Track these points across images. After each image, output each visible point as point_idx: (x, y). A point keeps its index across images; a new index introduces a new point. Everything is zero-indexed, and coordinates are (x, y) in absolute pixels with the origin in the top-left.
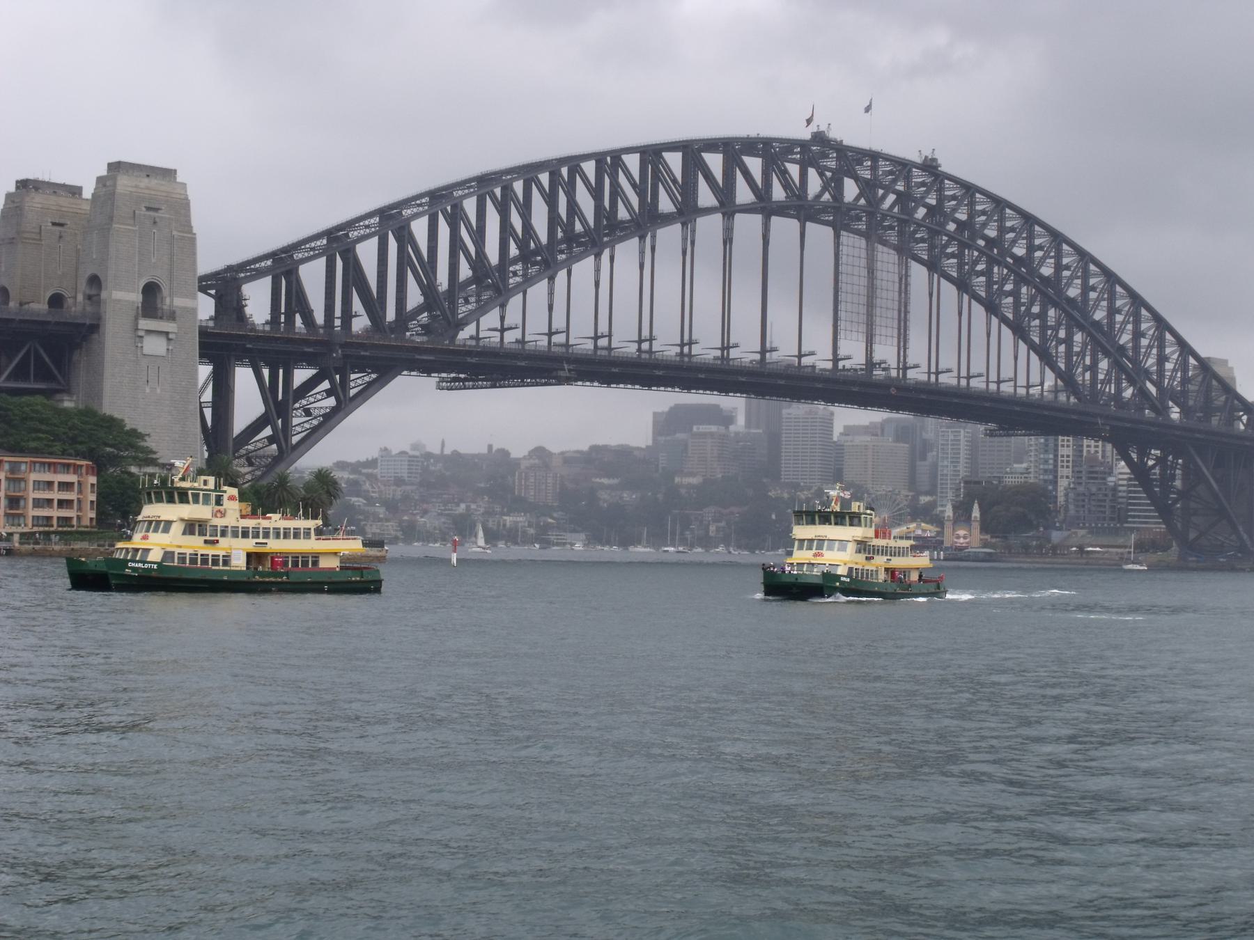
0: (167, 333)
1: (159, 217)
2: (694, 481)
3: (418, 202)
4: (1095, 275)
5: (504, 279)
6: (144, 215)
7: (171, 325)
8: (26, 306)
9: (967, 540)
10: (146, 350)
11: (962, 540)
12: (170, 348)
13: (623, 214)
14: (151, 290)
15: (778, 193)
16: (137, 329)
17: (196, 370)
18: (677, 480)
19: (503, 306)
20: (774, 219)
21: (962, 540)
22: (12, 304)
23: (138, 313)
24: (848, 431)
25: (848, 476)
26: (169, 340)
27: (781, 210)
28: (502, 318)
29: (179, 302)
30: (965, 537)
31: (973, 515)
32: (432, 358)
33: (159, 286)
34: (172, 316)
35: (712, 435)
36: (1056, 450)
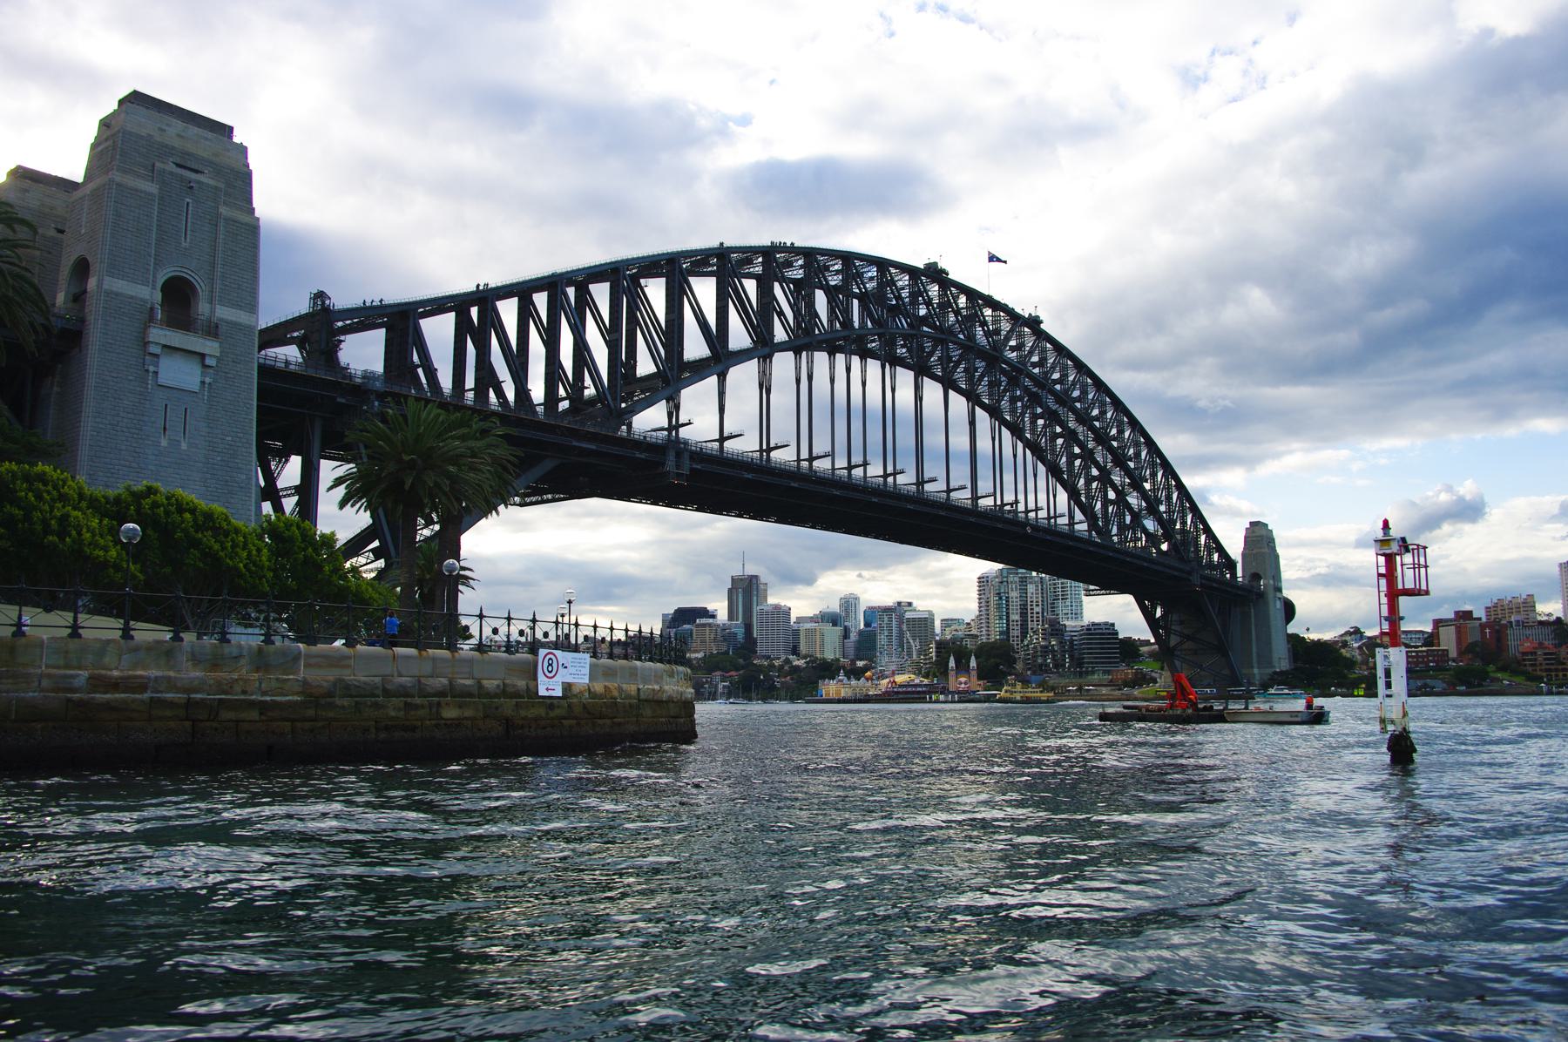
0: (203, 356)
1: (199, 182)
2: (700, 655)
6: (171, 173)
7: (209, 343)
10: (162, 380)
11: (963, 686)
12: (208, 380)
16: (146, 344)
18: (688, 655)
21: (963, 686)
24: (800, 620)
25: (803, 649)
26: (205, 366)
29: (224, 313)
31: (971, 665)
32: (594, 447)
35: (710, 625)
36: (1008, 617)
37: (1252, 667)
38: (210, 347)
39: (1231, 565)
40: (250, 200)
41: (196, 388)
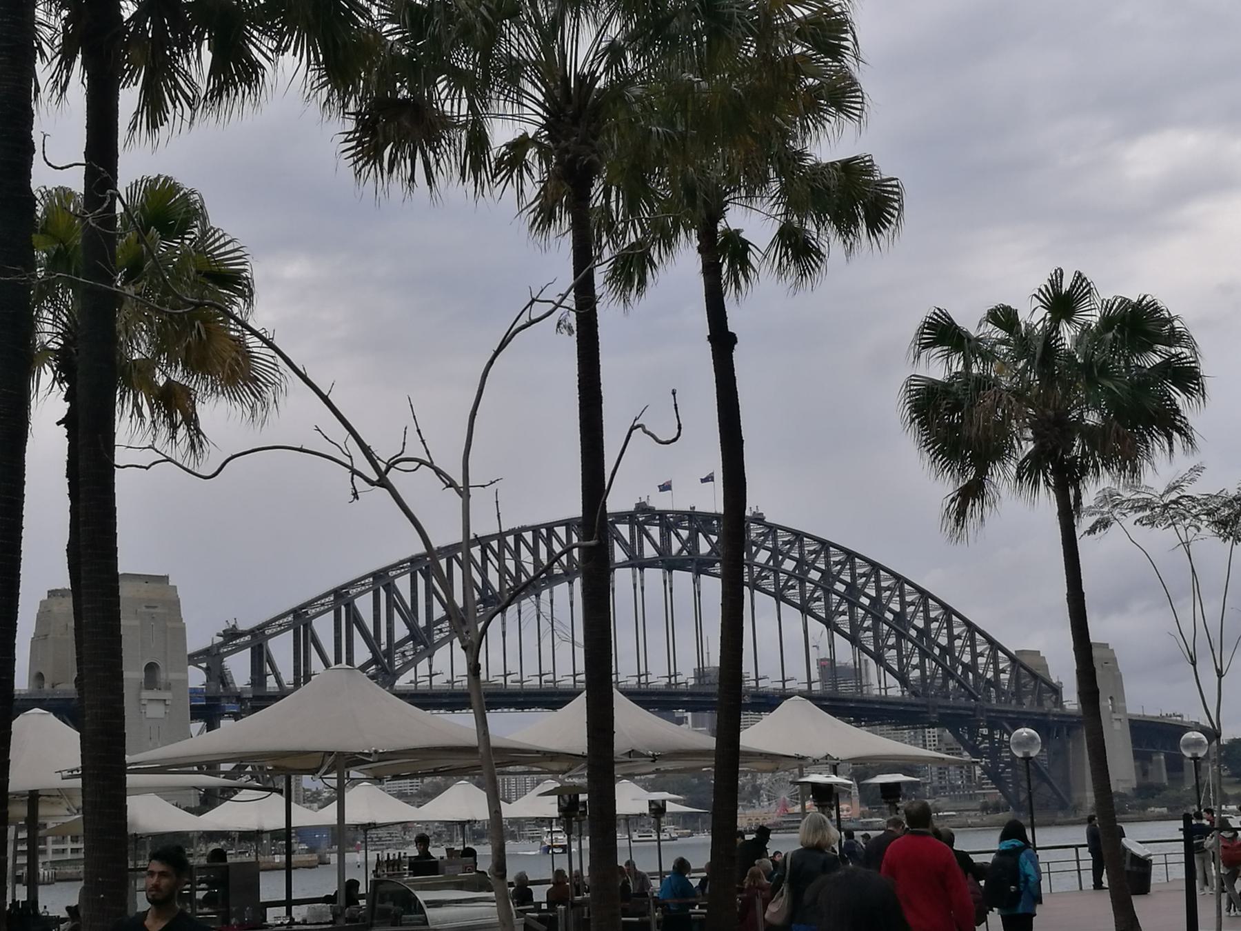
0: (165, 700)
3: (363, 582)
4: (910, 593)
5: (430, 636)
8: (58, 687)
9: (850, 813)
12: (168, 711)
13: (524, 579)
14: (151, 668)
15: (649, 552)
16: (140, 700)
17: (189, 727)
19: (430, 657)
20: (646, 569)
22: (47, 686)
23: (141, 688)
27: (652, 563)
28: (431, 667)
29: (173, 676)
30: (848, 811)
33: (158, 666)
34: (168, 687)
37: (1085, 791)
38: (167, 695)
39: (1056, 690)
40: (180, 615)
41: (163, 716)
